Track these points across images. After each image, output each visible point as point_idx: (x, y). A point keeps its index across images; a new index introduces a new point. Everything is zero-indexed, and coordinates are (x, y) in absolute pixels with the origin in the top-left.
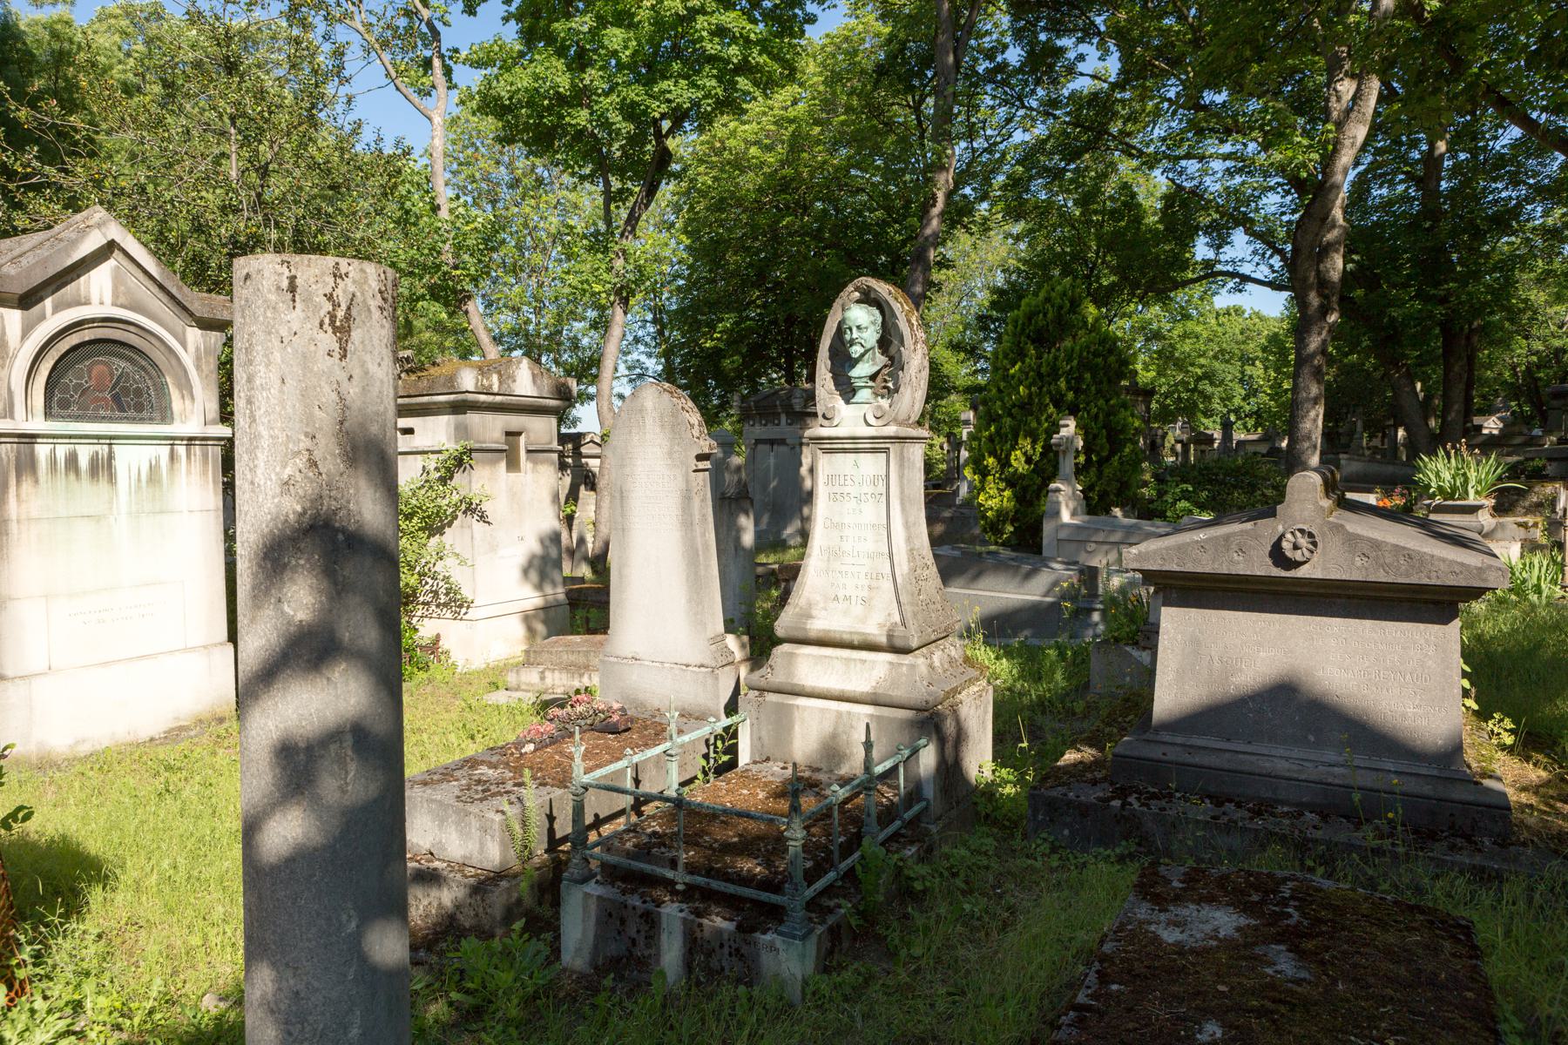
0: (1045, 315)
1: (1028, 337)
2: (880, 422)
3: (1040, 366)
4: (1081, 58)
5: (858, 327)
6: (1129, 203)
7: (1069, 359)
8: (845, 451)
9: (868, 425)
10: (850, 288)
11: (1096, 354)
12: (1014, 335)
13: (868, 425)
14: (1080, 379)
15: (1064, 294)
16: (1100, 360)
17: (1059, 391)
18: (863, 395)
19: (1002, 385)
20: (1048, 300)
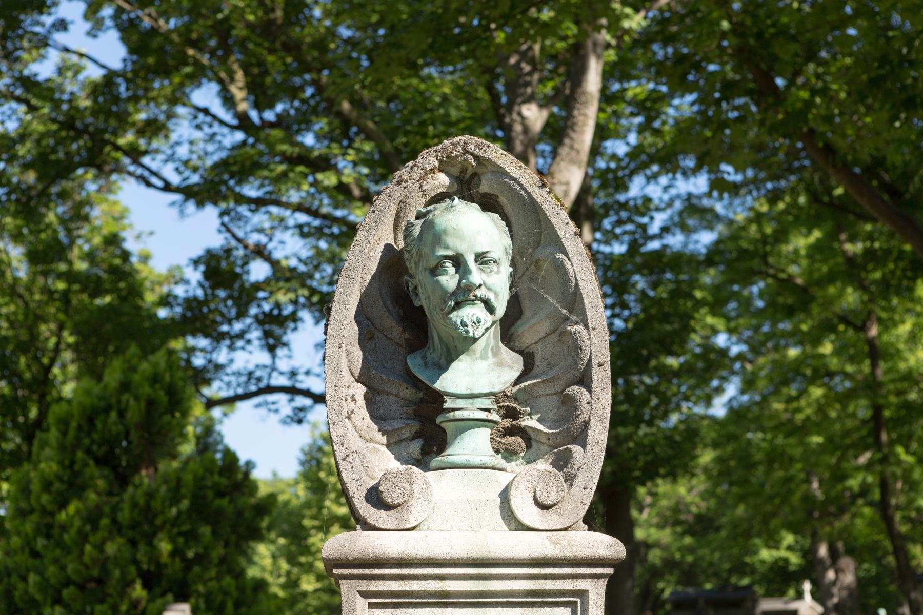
0: (121, 414)
1: (88, 451)
2: (552, 520)
3: (115, 509)
4: (62, 25)
5: (481, 258)
6: (117, 271)
7: (175, 499)
8: (443, 600)
9: (522, 527)
10: (429, 159)
11: (220, 494)
12: (62, 448)
13: (522, 527)
14: (192, 536)
15: (155, 379)
16: (224, 502)
17: (154, 559)
18: (474, 445)
19: (41, 542)
20: (125, 387)
